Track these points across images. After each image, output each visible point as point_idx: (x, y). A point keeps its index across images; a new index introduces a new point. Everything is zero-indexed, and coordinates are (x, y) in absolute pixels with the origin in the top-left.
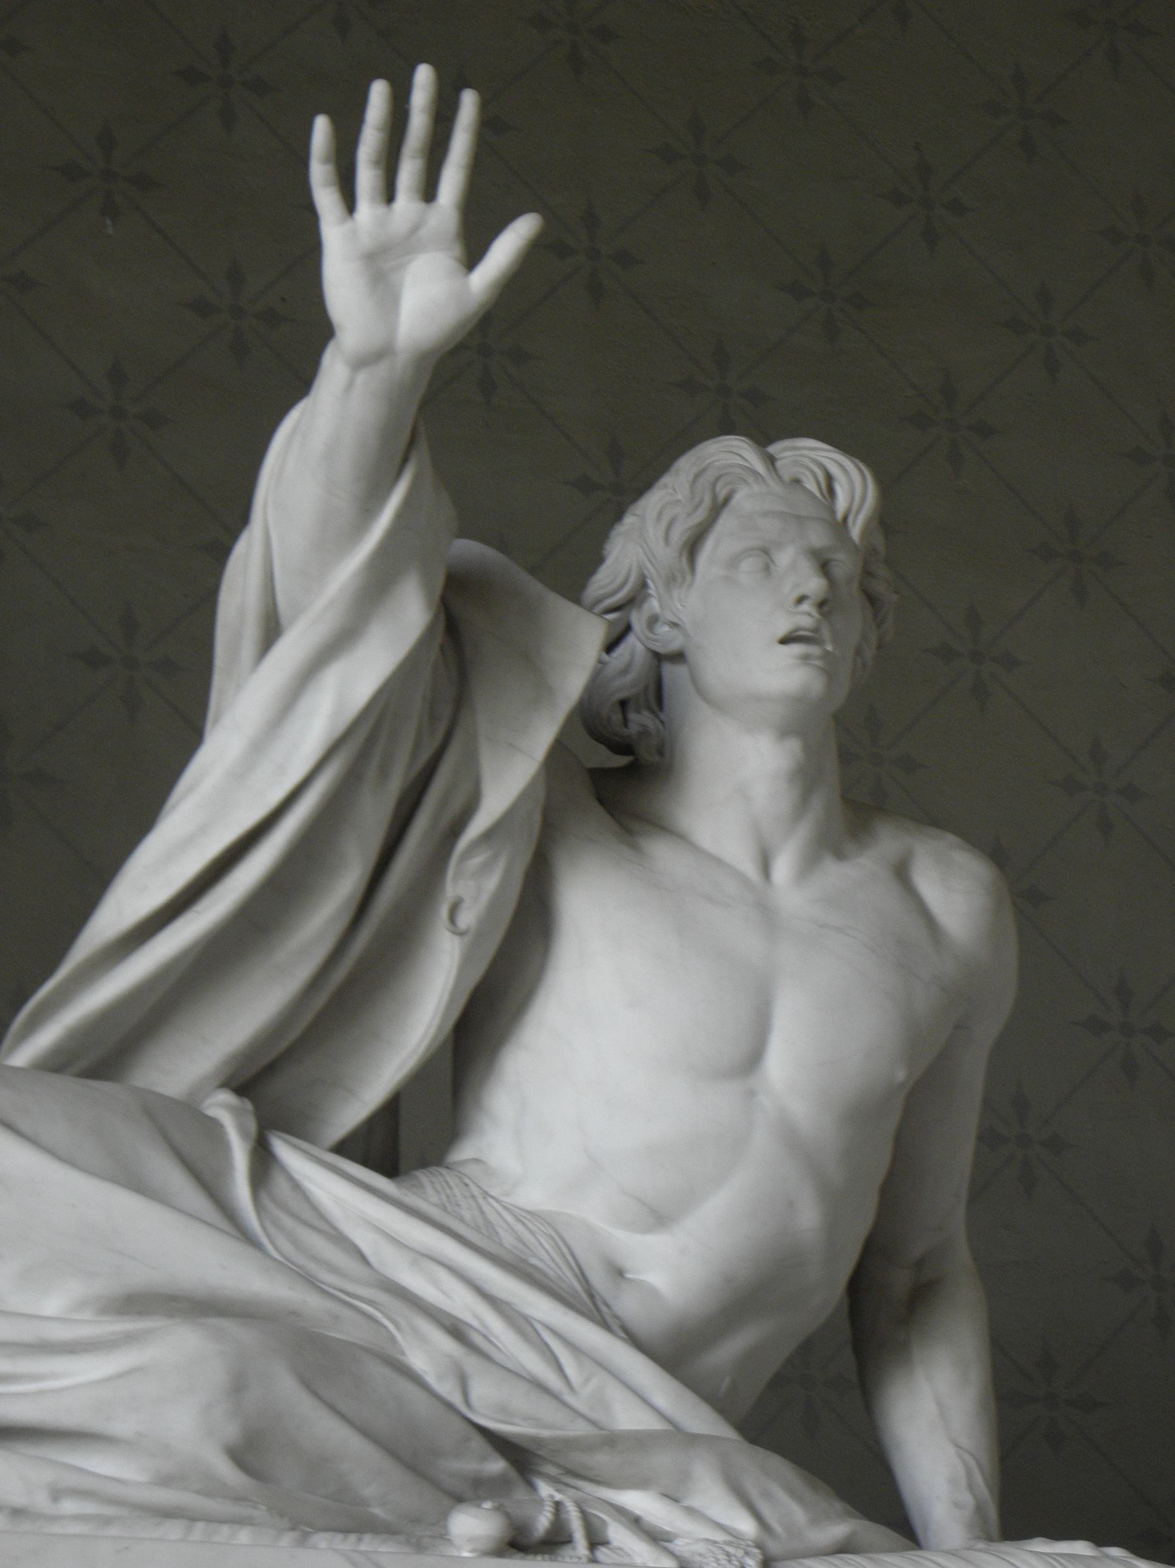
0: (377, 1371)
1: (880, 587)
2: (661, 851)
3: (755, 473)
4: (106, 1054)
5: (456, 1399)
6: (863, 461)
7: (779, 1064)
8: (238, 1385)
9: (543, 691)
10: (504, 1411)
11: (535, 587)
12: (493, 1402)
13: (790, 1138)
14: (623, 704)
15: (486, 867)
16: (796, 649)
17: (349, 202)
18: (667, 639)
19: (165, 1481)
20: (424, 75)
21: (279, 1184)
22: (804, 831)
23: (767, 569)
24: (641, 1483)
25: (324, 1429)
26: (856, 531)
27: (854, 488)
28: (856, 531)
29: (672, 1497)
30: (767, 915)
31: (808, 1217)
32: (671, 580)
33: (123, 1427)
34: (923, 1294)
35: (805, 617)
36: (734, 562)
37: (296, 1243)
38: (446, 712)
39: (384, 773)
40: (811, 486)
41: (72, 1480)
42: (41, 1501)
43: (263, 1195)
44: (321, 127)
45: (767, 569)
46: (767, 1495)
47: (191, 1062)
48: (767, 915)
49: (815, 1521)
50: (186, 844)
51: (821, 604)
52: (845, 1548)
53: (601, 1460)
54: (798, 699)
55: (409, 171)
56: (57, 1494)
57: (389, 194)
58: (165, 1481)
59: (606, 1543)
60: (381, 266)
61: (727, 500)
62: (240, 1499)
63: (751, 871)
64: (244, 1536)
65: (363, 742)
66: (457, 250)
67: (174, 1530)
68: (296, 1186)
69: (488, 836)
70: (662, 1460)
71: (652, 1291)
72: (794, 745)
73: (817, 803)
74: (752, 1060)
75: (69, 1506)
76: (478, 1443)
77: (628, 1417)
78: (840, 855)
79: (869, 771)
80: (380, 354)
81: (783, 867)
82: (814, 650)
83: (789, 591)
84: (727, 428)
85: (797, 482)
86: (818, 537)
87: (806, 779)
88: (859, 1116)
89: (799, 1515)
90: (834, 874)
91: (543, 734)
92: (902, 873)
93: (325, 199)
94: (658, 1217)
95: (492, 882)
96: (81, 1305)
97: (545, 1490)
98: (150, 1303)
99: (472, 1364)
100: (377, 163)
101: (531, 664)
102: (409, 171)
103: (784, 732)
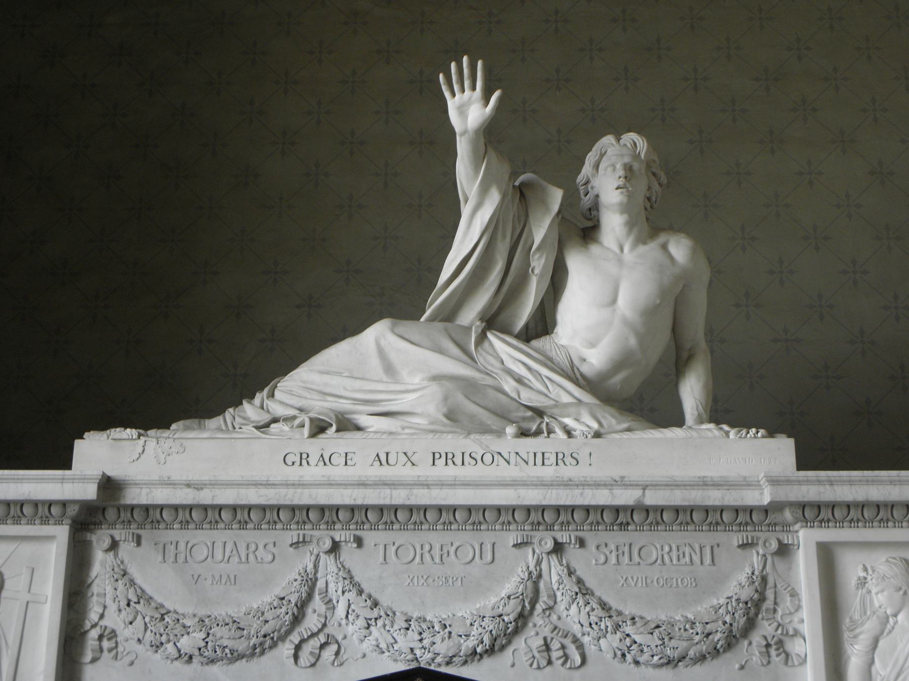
0: (492, 393)
1: (654, 170)
2: (594, 249)
3: (612, 144)
4: (448, 314)
5: (516, 397)
6: (645, 136)
7: (621, 301)
8: (446, 398)
9: (547, 210)
10: (530, 400)
11: (545, 183)
12: (526, 397)
13: (625, 322)
14: (590, 209)
15: (540, 257)
16: (619, 190)
17: (454, 95)
18: (595, 192)
19: (432, 423)
20: (465, 59)
21: (486, 344)
22: (631, 239)
23: (614, 170)
24: (568, 416)
25: (472, 408)
26: (643, 156)
27: (642, 144)
28: (643, 156)
29: (577, 420)
30: (620, 262)
31: (633, 342)
32: (593, 176)
33: (418, 410)
34: (690, 358)
35: (621, 182)
36: (606, 169)
37: (485, 359)
38: (523, 219)
39: (504, 236)
40: (629, 145)
41: (405, 424)
42: (399, 430)
43: (479, 349)
44: (441, 77)
45: (614, 170)
46: (604, 417)
47: (470, 315)
48: (620, 262)
49: (619, 423)
50: (453, 260)
51: (626, 177)
52: (629, 430)
53: (555, 411)
54: (621, 204)
55: (467, 83)
56: (403, 428)
57: (463, 91)
58: (432, 423)
59: (554, 432)
60: (462, 110)
61: (605, 153)
62: (445, 425)
63: (617, 250)
64: (450, 436)
65: (493, 229)
66: (482, 102)
67: (431, 436)
68: (491, 344)
69: (538, 249)
70: (572, 410)
71: (592, 364)
72: (625, 216)
73: (635, 231)
74: (614, 301)
75: (407, 431)
76: (522, 408)
77: (566, 399)
78: (645, 243)
79: (653, 218)
80: (465, 132)
81: (626, 249)
82: (624, 190)
83: (617, 176)
84: (629, 131)
85: (625, 145)
86: (627, 160)
87: (631, 225)
88: (650, 313)
89: (614, 421)
90: (642, 249)
91: (547, 221)
92: (664, 247)
93: (447, 94)
94: (592, 345)
95: (543, 261)
96: (423, 380)
97: (546, 419)
98: (437, 378)
99: (521, 388)
100: (457, 83)
101: (544, 203)
102: (467, 83)
103: (622, 213)
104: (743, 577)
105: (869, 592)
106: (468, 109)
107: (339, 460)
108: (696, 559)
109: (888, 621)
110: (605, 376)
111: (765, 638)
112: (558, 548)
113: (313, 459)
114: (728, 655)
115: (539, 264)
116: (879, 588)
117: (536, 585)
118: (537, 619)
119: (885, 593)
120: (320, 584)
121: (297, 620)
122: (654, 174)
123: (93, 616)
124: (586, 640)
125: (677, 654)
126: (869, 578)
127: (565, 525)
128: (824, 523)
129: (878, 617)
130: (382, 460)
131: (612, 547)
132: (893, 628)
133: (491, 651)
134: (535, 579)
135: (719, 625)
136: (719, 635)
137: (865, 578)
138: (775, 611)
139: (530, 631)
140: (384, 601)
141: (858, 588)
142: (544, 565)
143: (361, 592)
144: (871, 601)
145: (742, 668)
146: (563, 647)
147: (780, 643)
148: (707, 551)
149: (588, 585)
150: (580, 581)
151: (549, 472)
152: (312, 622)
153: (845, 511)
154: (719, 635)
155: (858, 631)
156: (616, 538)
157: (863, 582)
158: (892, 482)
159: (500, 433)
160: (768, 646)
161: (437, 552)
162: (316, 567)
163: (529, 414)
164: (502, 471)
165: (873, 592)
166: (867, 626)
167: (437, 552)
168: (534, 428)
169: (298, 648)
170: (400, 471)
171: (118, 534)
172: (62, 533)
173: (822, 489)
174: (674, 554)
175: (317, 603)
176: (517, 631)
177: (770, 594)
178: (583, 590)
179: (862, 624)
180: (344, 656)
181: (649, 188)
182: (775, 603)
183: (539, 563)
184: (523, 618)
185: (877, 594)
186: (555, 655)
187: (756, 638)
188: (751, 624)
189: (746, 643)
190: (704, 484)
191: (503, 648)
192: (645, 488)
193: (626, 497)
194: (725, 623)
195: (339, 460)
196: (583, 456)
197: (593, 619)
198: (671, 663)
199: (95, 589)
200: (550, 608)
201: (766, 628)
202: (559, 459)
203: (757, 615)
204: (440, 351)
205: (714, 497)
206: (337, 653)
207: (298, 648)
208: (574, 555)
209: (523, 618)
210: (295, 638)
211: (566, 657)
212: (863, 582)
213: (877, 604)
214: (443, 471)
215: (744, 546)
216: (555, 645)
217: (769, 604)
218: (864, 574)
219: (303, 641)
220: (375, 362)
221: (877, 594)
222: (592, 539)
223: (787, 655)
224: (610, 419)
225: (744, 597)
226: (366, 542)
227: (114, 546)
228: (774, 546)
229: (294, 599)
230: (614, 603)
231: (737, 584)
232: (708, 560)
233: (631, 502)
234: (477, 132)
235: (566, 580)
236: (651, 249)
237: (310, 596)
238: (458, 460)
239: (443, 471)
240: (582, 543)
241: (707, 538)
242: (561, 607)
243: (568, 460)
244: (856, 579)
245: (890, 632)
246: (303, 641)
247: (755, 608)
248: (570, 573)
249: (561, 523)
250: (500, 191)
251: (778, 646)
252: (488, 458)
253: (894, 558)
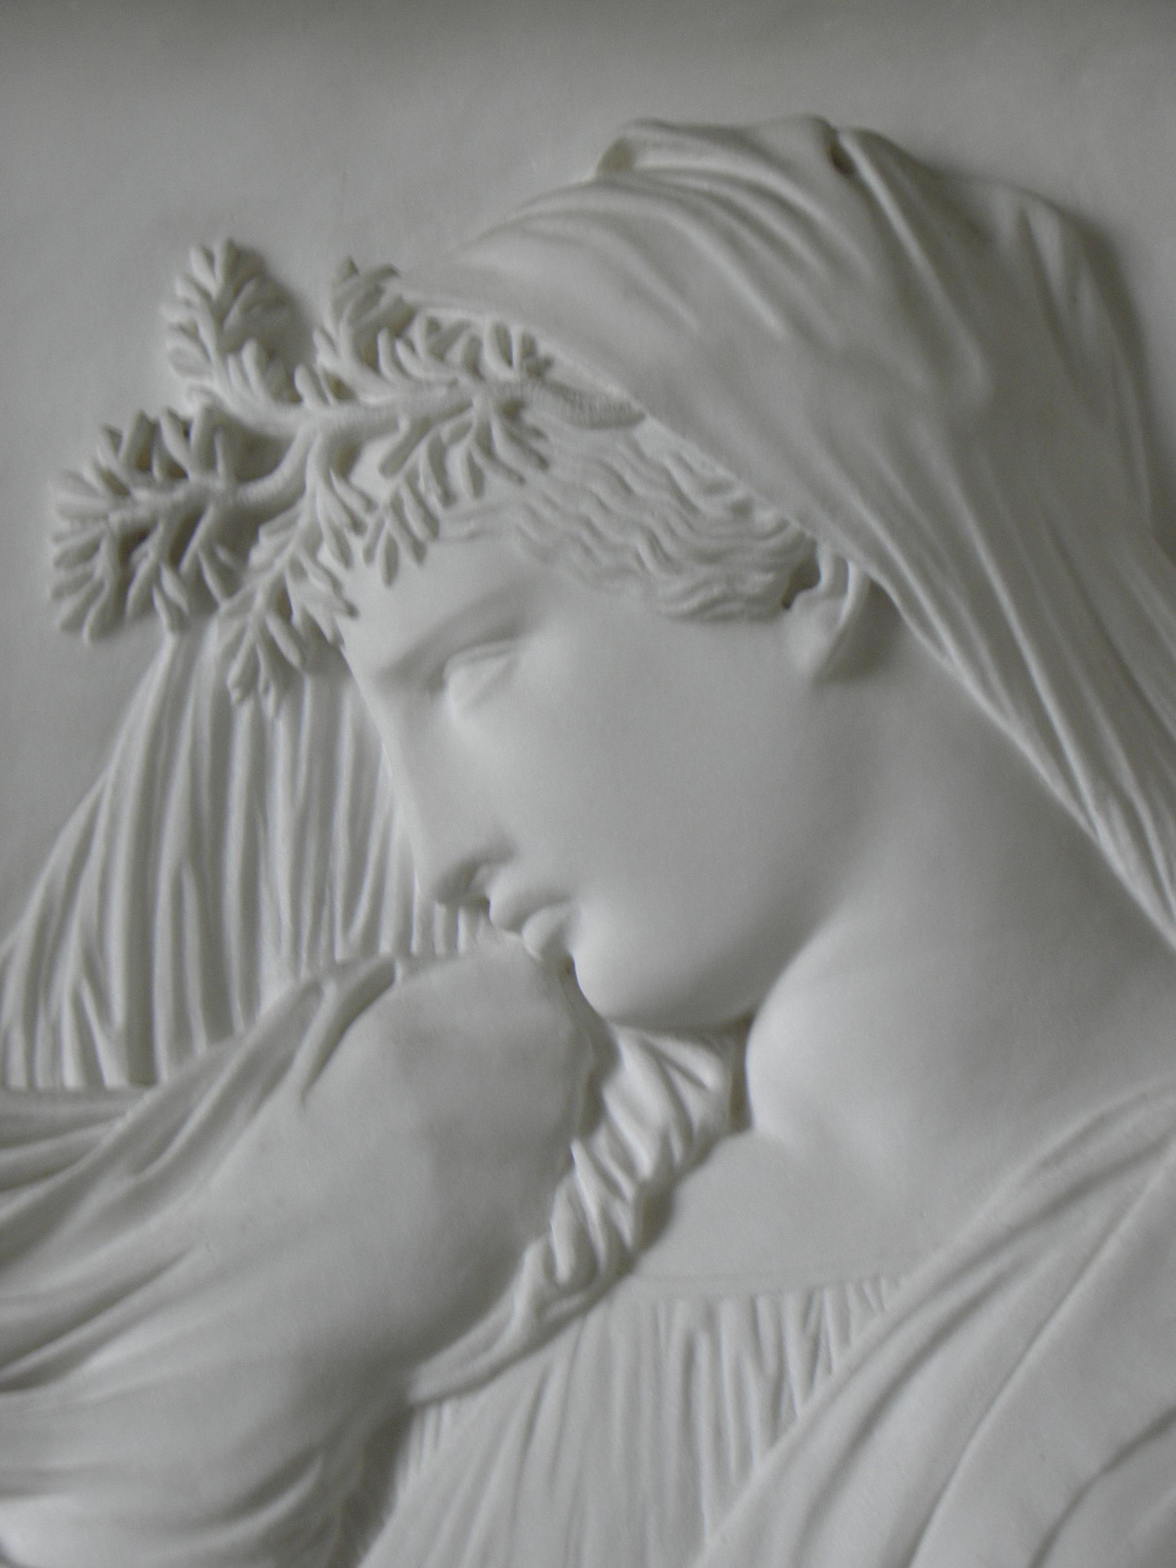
109: (592, 1114)
116: (442, 584)
119: (546, 654)
126: (309, 423)
129: (417, 1046)
132: (657, 1210)
137: (254, 452)
141: (117, 614)
144: (337, 799)
155: (63, 1273)
165: (367, 646)
166: (220, 1189)
179: (156, 1161)
185: (419, 675)
213: (412, 841)
218: (240, 389)
221: (419, 675)
244: (95, 456)
245: (600, 1274)
253: (737, 139)
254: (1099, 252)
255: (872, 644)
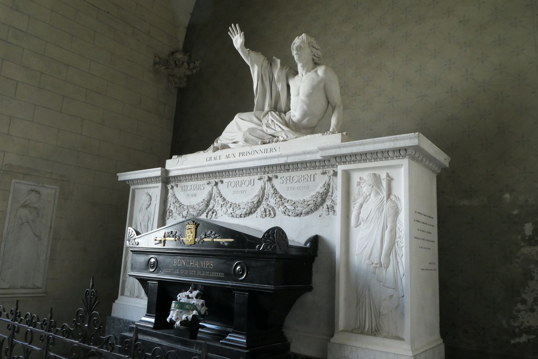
8: (244, 135)
11: (276, 59)
13: (302, 101)
31: (305, 107)
52: (296, 138)
65: (261, 78)
69: (278, 82)
73: (305, 68)
74: (298, 94)
78: (310, 72)
89: (292, 135)
90: (308, 74)
92: (316, 72)
99: (267, 129)
101: (276, 65)
104: (321, 185)
105: (361, 187)
106: (238, 40)
107: (218, 158)
108: (309, 179)
110: (300, 121)
111: (327, 205)
112: (270, 179)
113: (212, 159)
114: (316, 212)
115: (280, 87)
117: (264, 192)
118: (264, 202)
120: (213, 195)
121: (207, 206)
122: (313, 47)
123: (168, 207)
124: (276, 208)
125: (299, 212)
127: (272, 172)
128: (345, 163)
130: (228, 157)
131: (285, 178)
133: (250, 213)
134: (263, 189)
135: (312, 202)
136: (312, 205)
138: (332, 196)
139: (262, 206)
140: (227, 199)
142: (266, 185)
143: (221, 197)
144: (362, 190)
145: (320, 216)
146: (269, 211)
147: (333, 207)
148: (312, 177)
149: (278, 190)
150: (275, 190)
151: (268, 154)
152: (211, 206)
153: (349, 157)
154: (312, 205)
156: (287, 174)
157: (359, 184)
158: (360, 145)
159: (257, 144)
160: (328, 208)
161: (240, 184)
162: (212, 190)
163: (271, 137)
164: (256, 156)
167: (240, 184)
168: (268, 141)
169: (207, 214)
170: (232, 159)
171: (173, 184)
172: (160, 185)
173: (336, 150)
174: (302, 179)
175: (212, 201)
176: (258, 206)
177: (331, 190)
178: (276, 192)
179: (358, 199)
180: (218, 215)
181: (312, 52)
182: (332, 193)
183: (265, 184)
184: (259, 202)
186: (268, 213)
187: (325, 206)
188: (323, 201)
189: (322, 207)
190: (305, 153)
191: (254, 212)
192: (288, 156)
193: (282, 161)
194: (314, 201)
195: (218, 158)
196: (277, 149)
197: (277, 201)
198: (299, 215)
199: (169, 200)
200: (267, 199)
201: (328, 202)
202: (271, 150)
203: (326, 197)
204: (252, 122)
205: (308, 158)
206: (216, 215)
207: (207, 214)
208: (275, 182)
209: (259, 202)
210: (207, 211)
211: (270, 214)
212: (359, 184)
214: (242, 158)
215: (324, 173)
216: (267, 211)
217: (330, 194)
219: (208, 212)
220: (236, 128)
222: (280, 175)
223: (334, 211)
224: (291, 135)
225: (321, 192)
226: (224, 182)
227: (172, 188)
228: (332, 172)
229: (206, 199)
230: (284, 196)
231: (319, 188)
232: (312, 179)
233: (283, 162)
234: (241, 47)
235: (271, 188)
236: (311, 74)
237: (211, 199)
238: (245, 154)
239: (242, 158)
240: (276, 177)
241: (312, 172)
242: (270, 198)
243: (274, 150)
246: (208, 212)
247: (324, 196)
248: (273, 187)
249: (270, 171)
250: (258, 65)
251: (331, 209)
252: (253, 153)
254: (380, 176)
255: (373, 187)
